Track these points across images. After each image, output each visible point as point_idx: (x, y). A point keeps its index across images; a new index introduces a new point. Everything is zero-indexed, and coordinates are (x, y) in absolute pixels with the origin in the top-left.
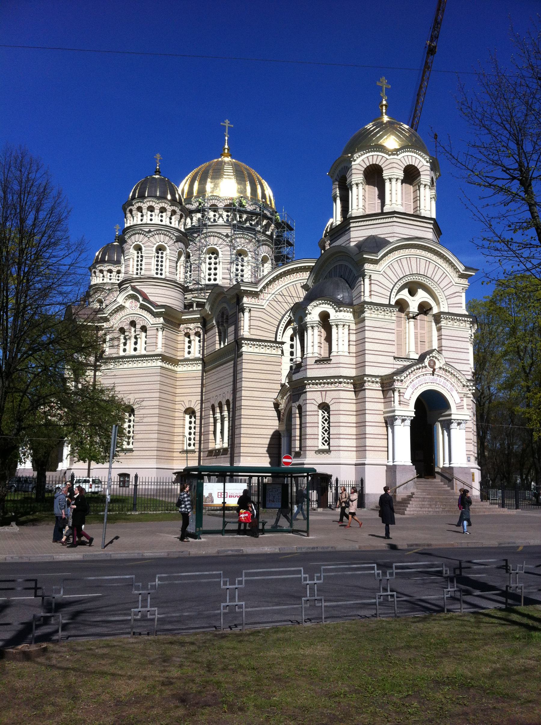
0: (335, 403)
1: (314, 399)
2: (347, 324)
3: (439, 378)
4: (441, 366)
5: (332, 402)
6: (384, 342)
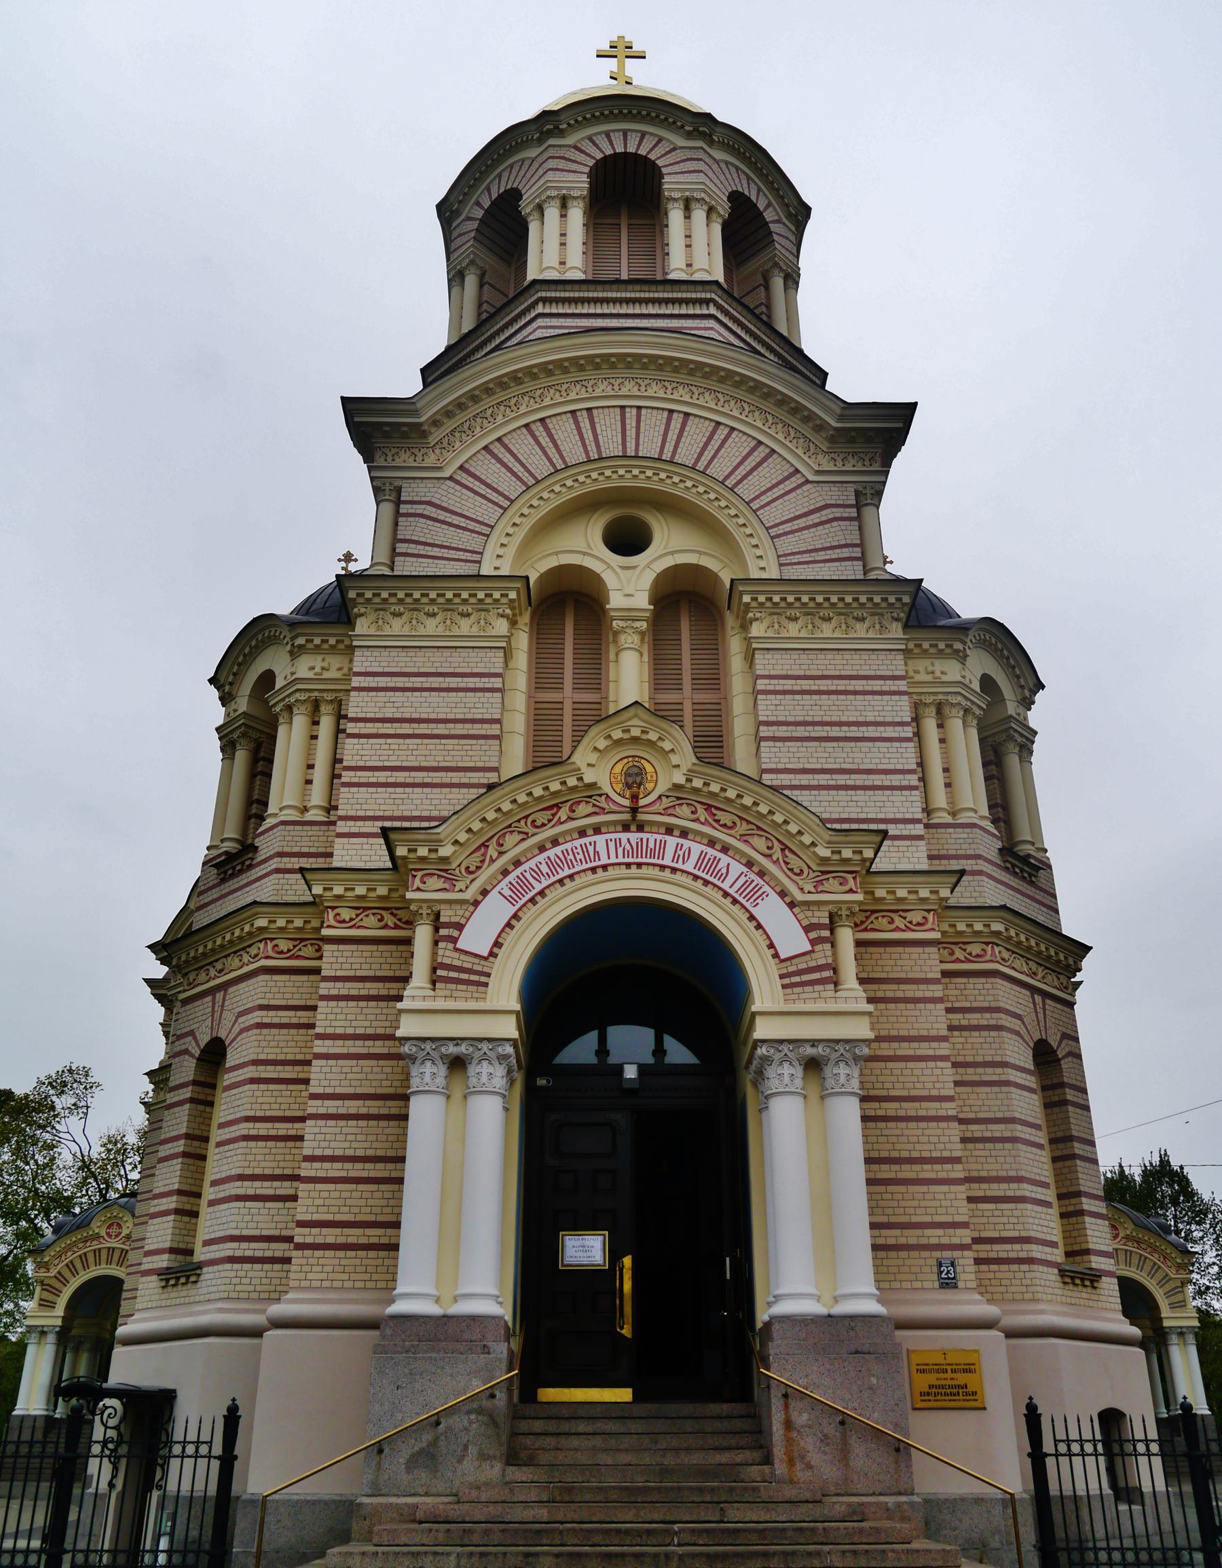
0: (242, 1031)
1: (191, 1033)
2: (329, 696)
3: (672, 841)
4: (680, 779)
5: (236, 1029)
6: (441, 729)
